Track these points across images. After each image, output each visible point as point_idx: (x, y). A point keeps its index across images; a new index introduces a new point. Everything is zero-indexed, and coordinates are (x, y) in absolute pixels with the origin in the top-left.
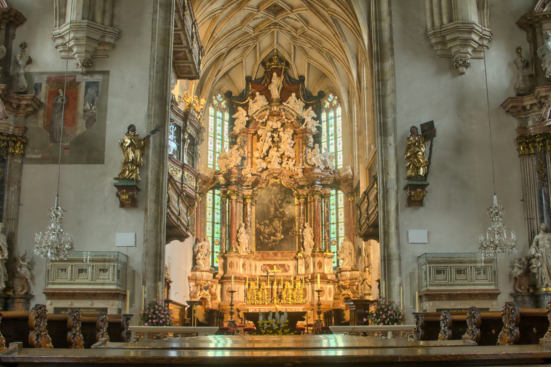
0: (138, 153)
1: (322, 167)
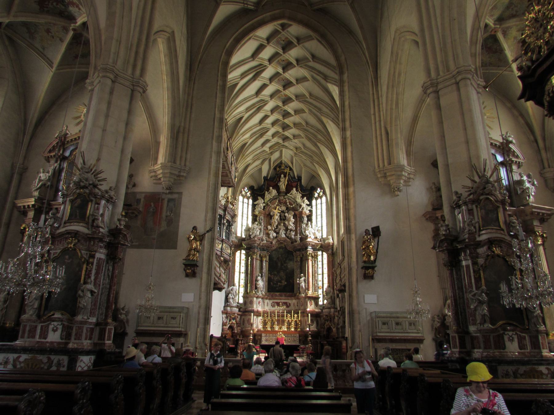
0: (198, 243)
1: (313, 237)
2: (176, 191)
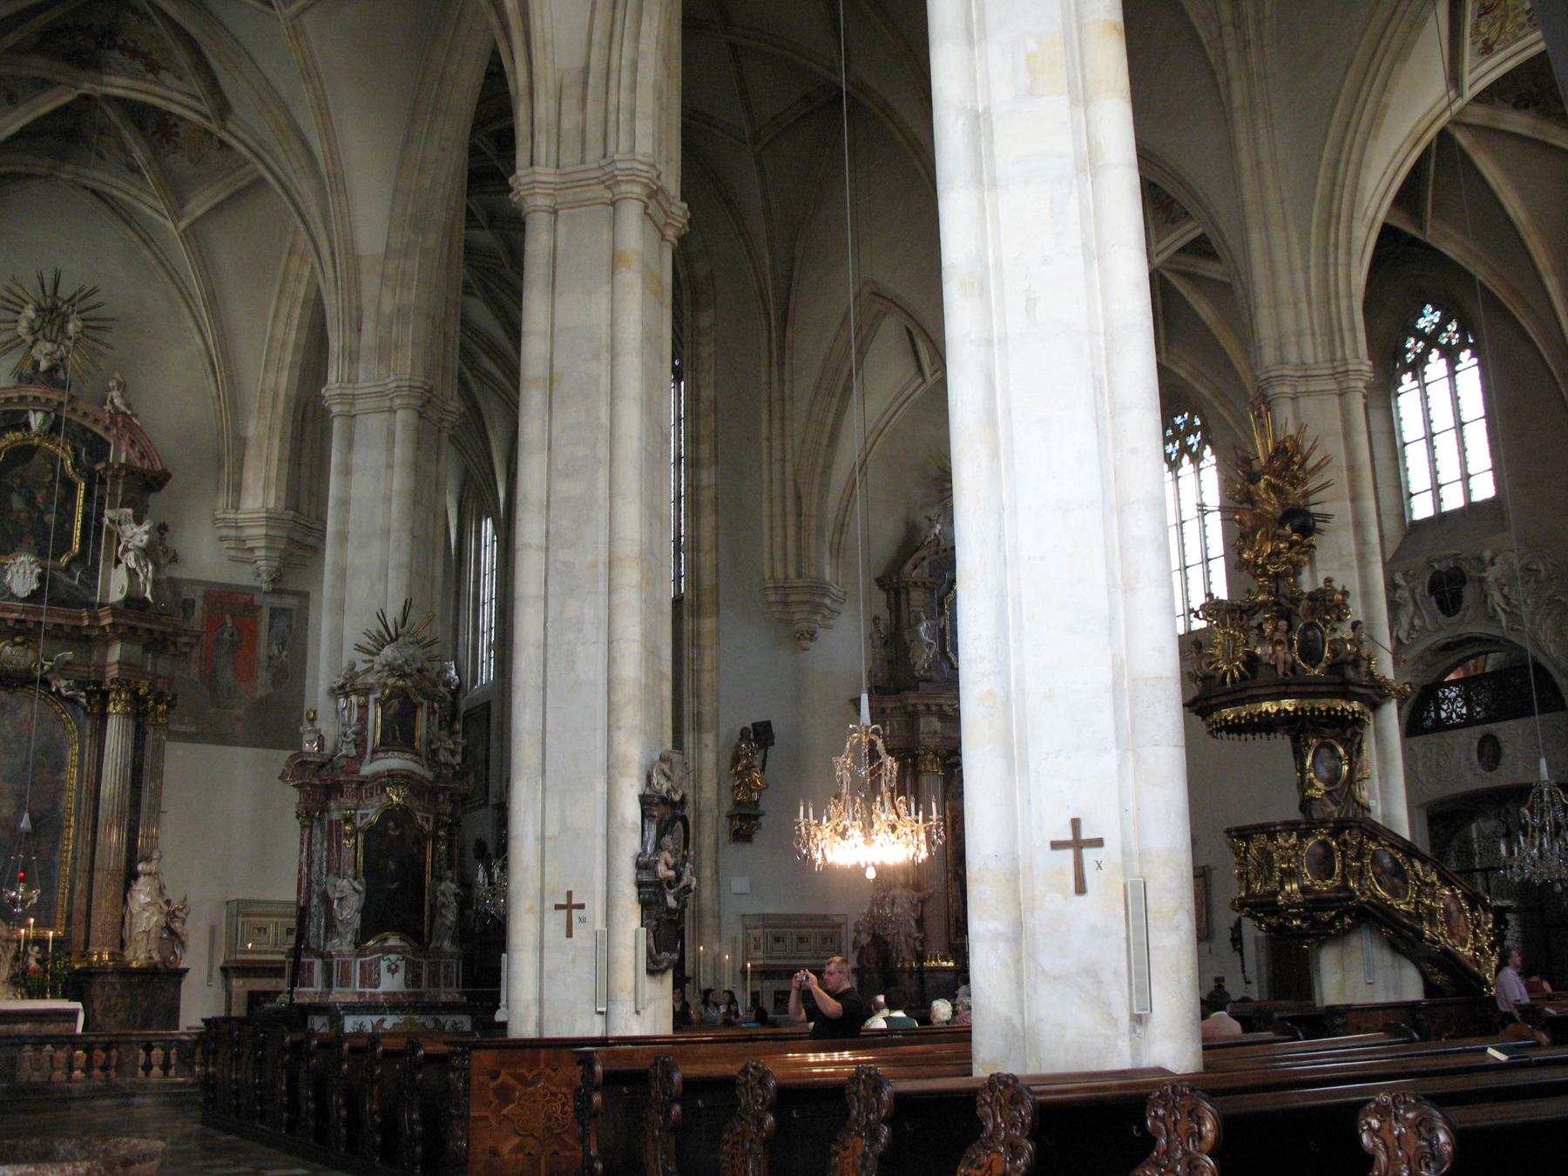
2: (291, 585)
